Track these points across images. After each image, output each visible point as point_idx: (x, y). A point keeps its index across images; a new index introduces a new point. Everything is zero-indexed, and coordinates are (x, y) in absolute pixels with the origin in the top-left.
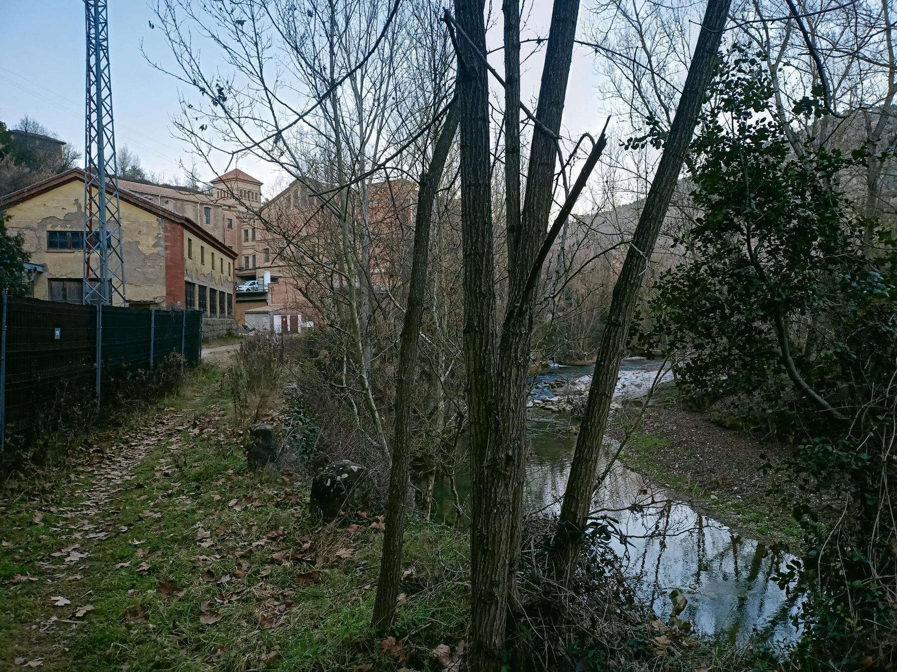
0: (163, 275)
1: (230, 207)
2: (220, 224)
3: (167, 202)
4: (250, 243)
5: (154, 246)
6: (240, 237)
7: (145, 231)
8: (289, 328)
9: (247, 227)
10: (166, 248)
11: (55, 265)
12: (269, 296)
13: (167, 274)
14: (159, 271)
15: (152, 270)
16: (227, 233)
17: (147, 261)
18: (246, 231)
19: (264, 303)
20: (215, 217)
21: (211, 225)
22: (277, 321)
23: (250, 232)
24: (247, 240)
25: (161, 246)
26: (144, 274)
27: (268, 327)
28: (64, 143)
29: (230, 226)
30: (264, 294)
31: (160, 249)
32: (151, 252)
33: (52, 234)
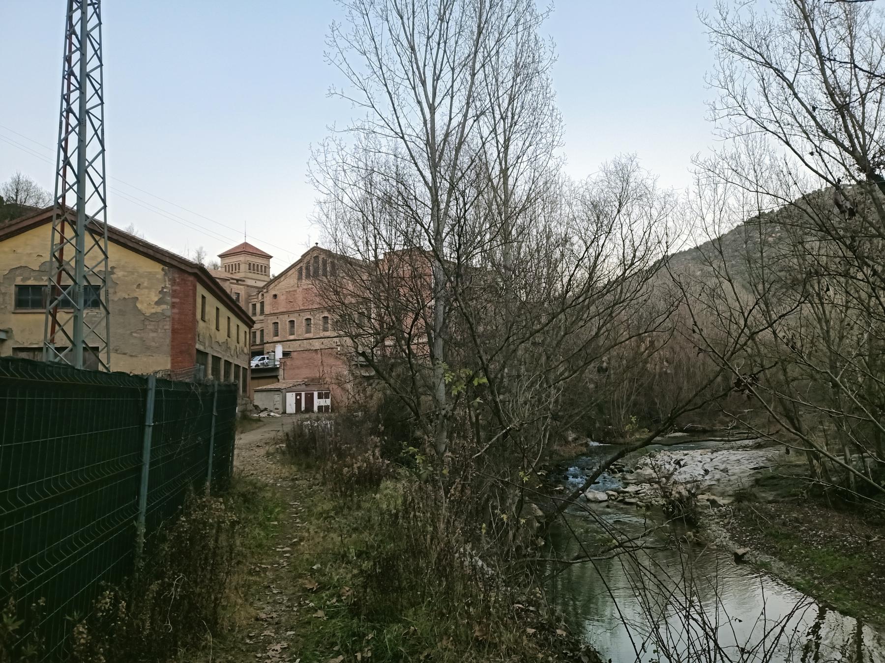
0: (168, 341)
1: (238, 280)
5: (158, 303)
7: (145, 284)
9: (254, 301)
10: (173, 306)
11: (23, 331)
12: (281, 372)
13: (173, 340)
14: (161, 335)
15: (155, 335)
17: (147, 323)
18: (254, 305)
22: (291, 398)
23: (258, 306)
25: (166, 303)
26: (142, 339)
27: (280, 407)
30: (275, 369)
31: (164, 307)
32: (153, 311)
33: (22, 289)
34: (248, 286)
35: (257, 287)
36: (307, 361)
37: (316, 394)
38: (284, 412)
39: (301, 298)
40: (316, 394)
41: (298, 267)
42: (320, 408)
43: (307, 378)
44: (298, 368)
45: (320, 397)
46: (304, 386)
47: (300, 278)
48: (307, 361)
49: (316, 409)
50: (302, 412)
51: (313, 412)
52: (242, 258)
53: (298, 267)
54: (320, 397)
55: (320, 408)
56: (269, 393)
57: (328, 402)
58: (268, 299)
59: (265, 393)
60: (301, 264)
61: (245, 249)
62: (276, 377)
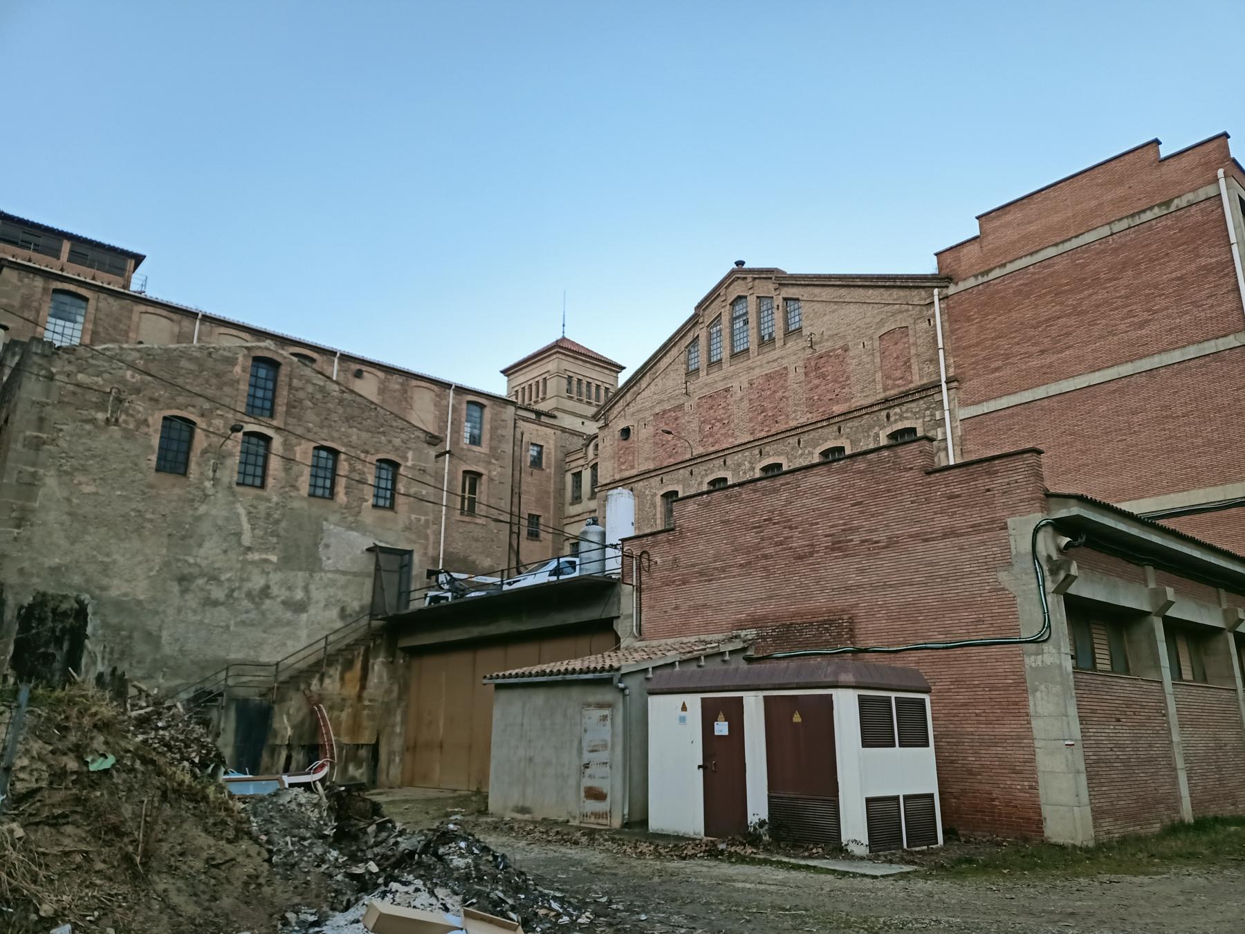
1: (539, 414)
2: (508, 448)
3: (358, 374)
4: (587, 505)
6: (560, 491)
8: (757, 807)
12: (627, 600)
16: (526, 479)
18: (577, 476)
19: (598, 640)
20: (494, 429)
21: (484, 449)
22: (675, 728)
24: (577, 499)
27: (612, 782)
28: (139, 259)
29: (537, 462)
34: (564, 430)
35: (580, 434)
36: (751, 538)
37: (846, 708)
38: (637, 823)
39: (694, 425)
40: (846, 708)
41: (689, 338)
42: (880, 811)
43: (755, 622)
44: (705, 575)
45: (875, 733)
46: (740, 663)
47: (691, 373)
48: (751, 538)
49: (854, 826)
50: (753, 839)
51: (838, 850)
52: (551, 365)
53: (689, 338)
54: (875, 733)
55: (880, 811)
56: (559, 694)
57: (911, 772)
58: (609, 442)
59: (539, 698)
60: (697, 331)
61: (562, 348)
62: (605, 627)
